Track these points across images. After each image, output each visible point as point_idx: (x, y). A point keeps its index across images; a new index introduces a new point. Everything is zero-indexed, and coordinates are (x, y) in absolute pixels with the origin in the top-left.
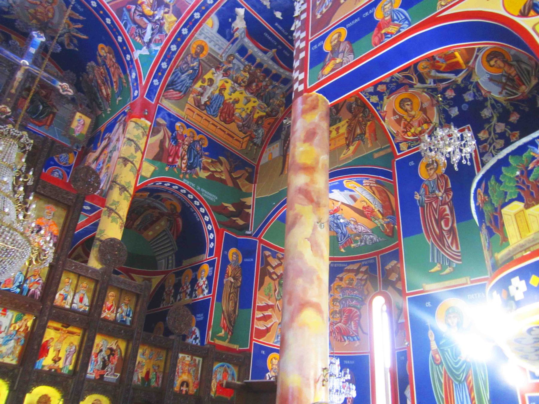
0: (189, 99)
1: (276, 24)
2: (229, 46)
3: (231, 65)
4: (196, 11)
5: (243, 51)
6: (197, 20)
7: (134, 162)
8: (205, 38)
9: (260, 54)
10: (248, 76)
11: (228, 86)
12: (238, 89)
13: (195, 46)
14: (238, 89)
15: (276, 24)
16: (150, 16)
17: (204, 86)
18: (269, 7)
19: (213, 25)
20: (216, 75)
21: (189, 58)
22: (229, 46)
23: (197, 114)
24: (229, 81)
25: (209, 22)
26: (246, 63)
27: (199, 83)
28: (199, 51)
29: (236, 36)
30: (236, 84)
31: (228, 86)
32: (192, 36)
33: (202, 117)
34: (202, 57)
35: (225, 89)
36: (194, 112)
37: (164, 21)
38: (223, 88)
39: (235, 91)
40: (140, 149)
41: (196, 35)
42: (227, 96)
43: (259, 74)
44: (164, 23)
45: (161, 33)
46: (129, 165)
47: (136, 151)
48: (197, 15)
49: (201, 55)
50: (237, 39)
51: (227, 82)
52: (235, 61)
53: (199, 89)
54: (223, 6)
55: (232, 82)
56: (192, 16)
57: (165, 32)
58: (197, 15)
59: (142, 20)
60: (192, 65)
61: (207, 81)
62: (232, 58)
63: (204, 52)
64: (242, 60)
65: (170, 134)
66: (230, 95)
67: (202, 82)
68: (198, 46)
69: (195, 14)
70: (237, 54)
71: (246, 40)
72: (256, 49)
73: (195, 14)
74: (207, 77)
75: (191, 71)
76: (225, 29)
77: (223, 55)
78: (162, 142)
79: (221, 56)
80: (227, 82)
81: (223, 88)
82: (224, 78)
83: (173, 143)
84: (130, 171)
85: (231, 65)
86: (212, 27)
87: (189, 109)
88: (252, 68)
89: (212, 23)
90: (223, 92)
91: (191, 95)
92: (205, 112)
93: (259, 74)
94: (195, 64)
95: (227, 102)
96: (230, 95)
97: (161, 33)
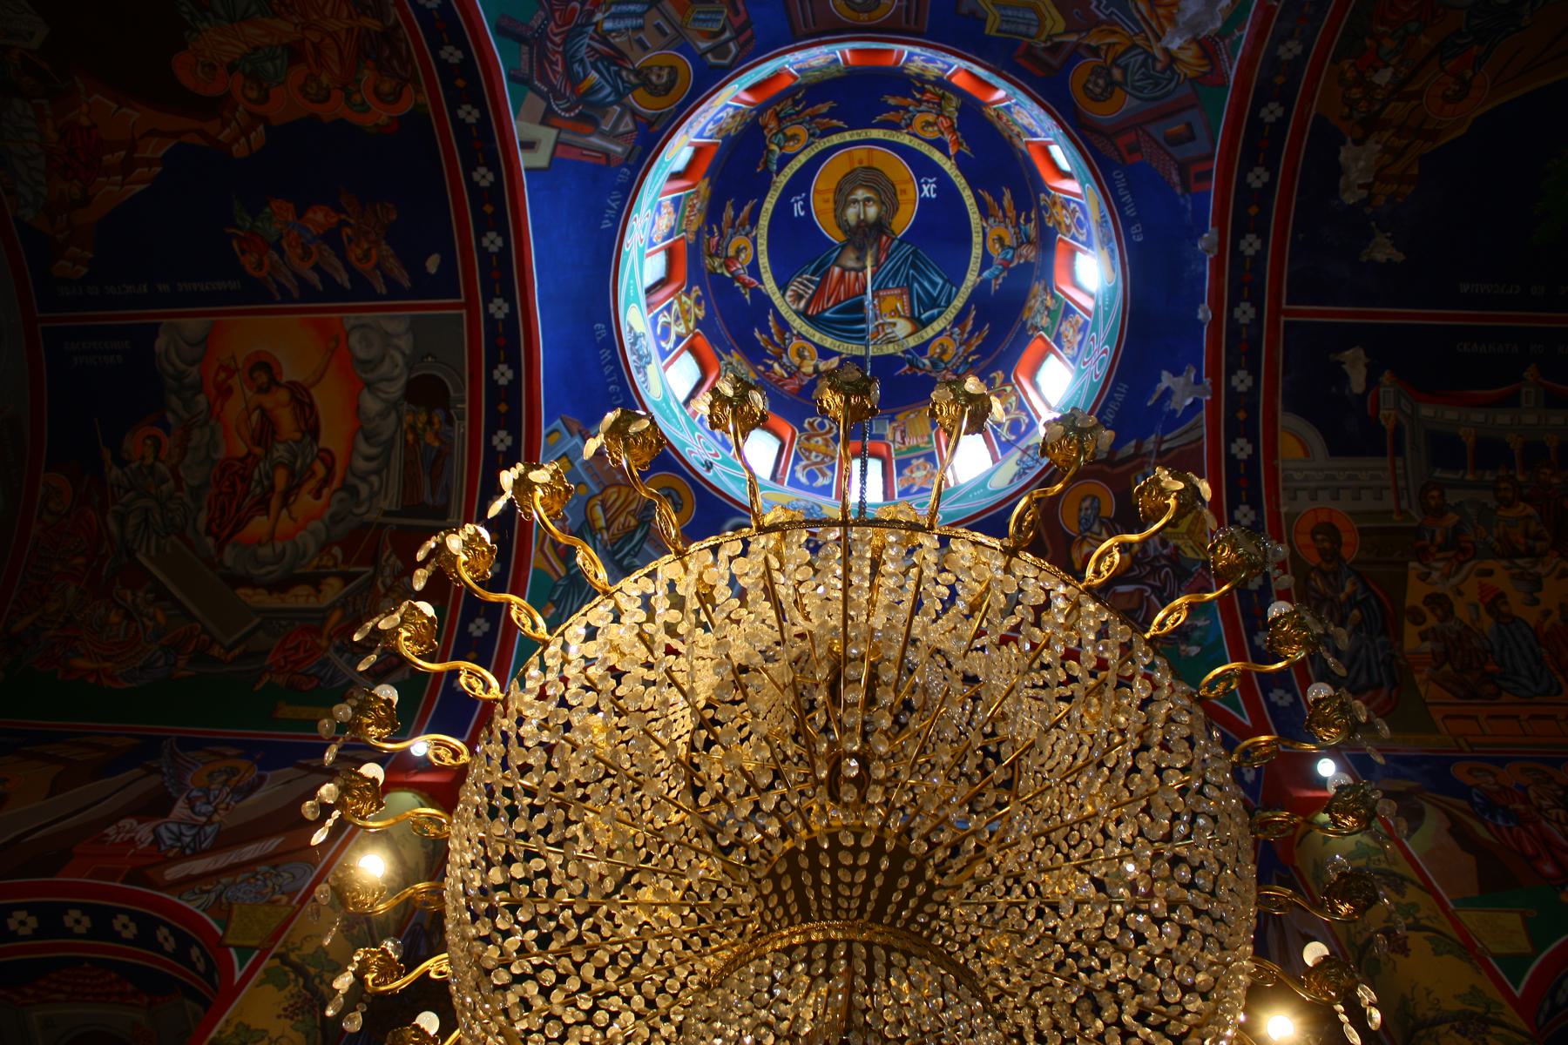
0: (1422, 690)
1: (1464, 288)
2: (1394, 467)
3: (1452, 518)
4: (1230, 440)
5: (1445, 449)
6: (1253, 460)
7: (1423, 922)
8: (1314, 498)
9: (1503, 418)
10: (1530, 510)
11: (1501, 579)
12: (1540, 569)
13: (1306, 539)
14: (1540, 569)
15: (1464, 288)
16: (1130, 569)
17: (1433, 629)
18: (1399, 257)
19: (1299, 441)
20: (1435, 575)
21: (1319, 583)
22: (1394, 467)
23: (1490, 717)
24: (1489, 564)
25: (1288, 447)
26: (1489, 476)
27: (1411, 632)
28: (1327, 545)
29: (1389, 425)
30: (1519, 561)
31: (1501, 579)
32: (1275, 516)
33: (1517, 717)
34: (1349, 553)
35: (1502, 595)
36: (1475, 718)
37: (1172, 543)
38: (1494, 601)
39: (1537, 583)
40: (1403, 879)
41: (1283, 510)
42: (1531, 616)
43: (1555, 480)
44: (1177, 548)
45: (1190, 574)
46: (1416, 940)
47: (1399, 890)
48: (1242, 449)
49: (1344, 552)
50: (1398, 429)
51: (1490, 573)
52: (1453, 497)
53: (1427, 646)
54: (1284, 373)
55: (1505, 563)
56: (1231, 457)
57: (1194, 562)
58: (1242, 449)
59: (1116, 594)
60: (1342, 596)
61: (1425, 609)
62: (1435, 493)
63: (1345, 538)
64: (1469, 477)
65: (1463, 803)
66: (1536, 602)
67: (1416, 623)
68: (1313, 534)
69: (1235, 449)
70: (1437, 473)
71: (1426, 411)
72: (1478, 416)
73: (1235, 449)
74: (1415, 594)
75: (1356, 612)
76: (1350, 430)
77: (1404, 504)
78: (1458, 831)
79: (1401, 512)
80: (1490, 573)
81: (1494, 601)
82: (1467, 567)
83: (1500, 822)
84: (1436, 953)
85: (1452, 518)
86: (1307, 453)
87: (1446, 717)
88: (1520, 478)
89: (1297, 445)
90: (1504, 609)
91: (1417, 678)
92: (1505, 697)
93: (1555, 480)
94: (1348, 588)
95: (1547, 625)
96: (1536, 602)
97: (1190, 574)
